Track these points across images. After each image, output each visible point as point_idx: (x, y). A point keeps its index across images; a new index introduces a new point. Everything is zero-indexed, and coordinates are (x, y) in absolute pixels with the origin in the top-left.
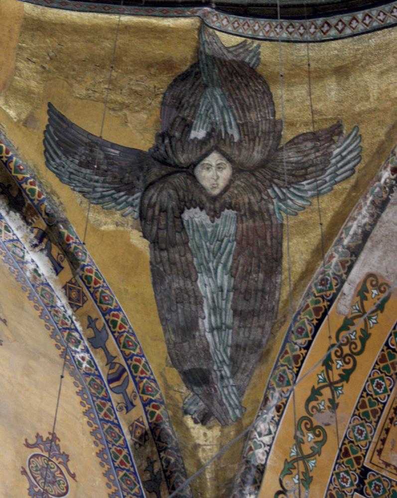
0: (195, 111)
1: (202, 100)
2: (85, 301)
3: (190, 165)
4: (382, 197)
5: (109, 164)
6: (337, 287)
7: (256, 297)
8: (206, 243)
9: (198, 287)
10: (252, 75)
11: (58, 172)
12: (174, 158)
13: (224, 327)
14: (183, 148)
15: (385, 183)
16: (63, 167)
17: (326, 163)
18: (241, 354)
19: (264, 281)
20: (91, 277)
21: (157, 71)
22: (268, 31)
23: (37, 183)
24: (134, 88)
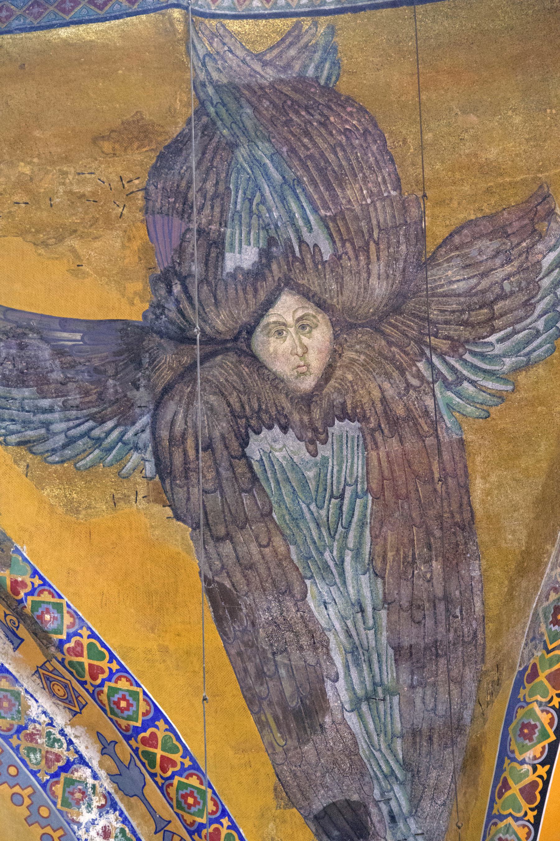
0: (222, 205)
1: (234, 176)
2: (84, 706)
3: (240, 333)
7: (435, 613)
8: (308, 506)
9: (310, 611)
10: (330, 100)
13: (380, 690)
18: (424, 750)
19: (446, 580)
20: (81, 664)
21: (117, 146)
24: (76, 189)
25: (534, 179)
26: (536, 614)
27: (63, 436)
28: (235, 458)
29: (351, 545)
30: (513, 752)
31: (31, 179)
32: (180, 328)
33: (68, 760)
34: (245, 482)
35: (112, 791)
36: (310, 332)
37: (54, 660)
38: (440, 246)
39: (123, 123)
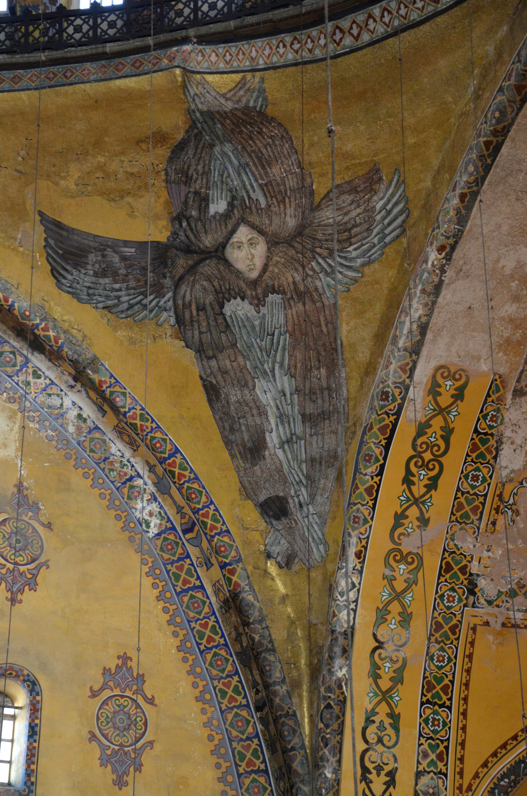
0: (207, 179)
3: (218, 248)
4: (433, 281)
6: (401, 396)
8: (256, 340)
9: (257, 395)
11: (74, 290)
12: (199, 243)
13: (294, 437)
14: (205, 228)
15: (433, 265)
16: (78, 284)
17: (370, 221)
19: (328, 377)
20: (136, 424)
22: (269, 55)
23: (51, 324)
24: (129, 170)
25: (372, 161)
26: (373, 396)
27: (127, 304)
28: (218, 314)
29: (278, 360)
30: (360, 469)
31: (105, 165)
33: (131, 476)
34: (222, 328)
35: (154, 491)
38: (322, 199)
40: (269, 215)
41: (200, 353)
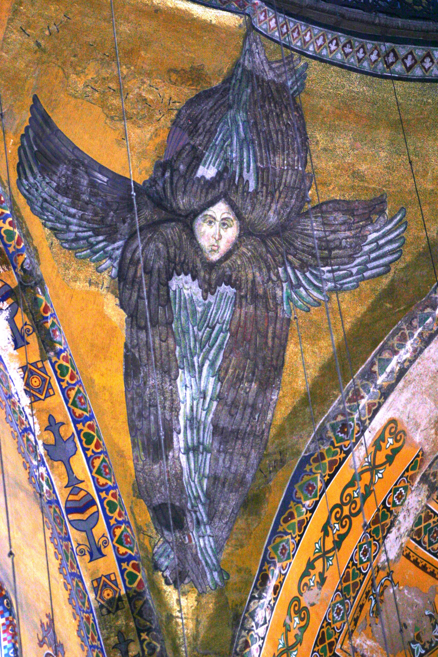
2: (51, 396)
5: (92, 195)
7: (243, 414)
8: (193, 327)
9: (177, 387)
11: (30, 196)
12: (172, 200)
13: (201, 447)
16: (37, 190)
18: (219, 489)
19: (257, 395)
21: (179, 79)
22: (321, 46)
25: (380, 190)
27: (73, 234)
28: (162, 284)
29: (210, 358)
32: (160, 198)
34: (163, 300)
35: (43, 454)
36: (226, 228)
37: (48, 361)
39: (191, 67)
40: (253, 202)
41: (132, 319)
